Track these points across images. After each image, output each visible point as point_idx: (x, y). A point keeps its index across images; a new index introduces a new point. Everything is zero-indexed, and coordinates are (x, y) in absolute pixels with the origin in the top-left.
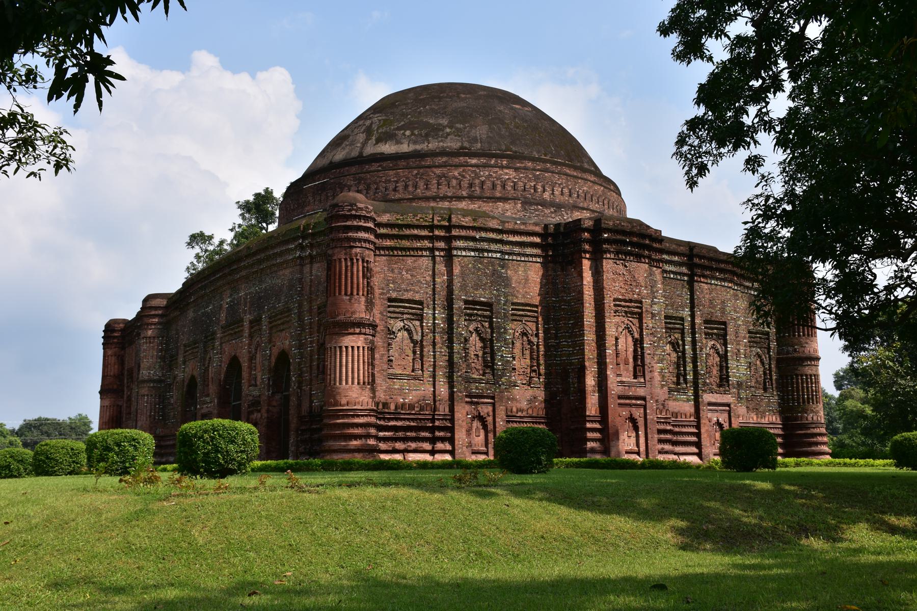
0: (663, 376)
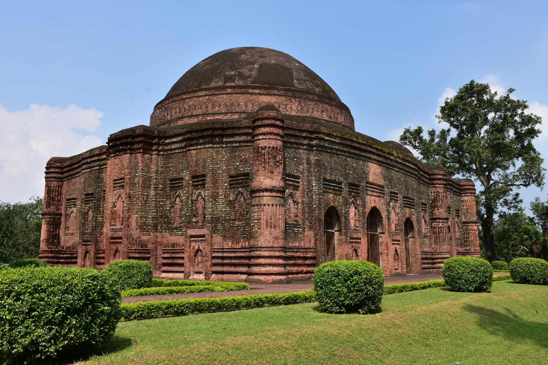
0: (137, 223)
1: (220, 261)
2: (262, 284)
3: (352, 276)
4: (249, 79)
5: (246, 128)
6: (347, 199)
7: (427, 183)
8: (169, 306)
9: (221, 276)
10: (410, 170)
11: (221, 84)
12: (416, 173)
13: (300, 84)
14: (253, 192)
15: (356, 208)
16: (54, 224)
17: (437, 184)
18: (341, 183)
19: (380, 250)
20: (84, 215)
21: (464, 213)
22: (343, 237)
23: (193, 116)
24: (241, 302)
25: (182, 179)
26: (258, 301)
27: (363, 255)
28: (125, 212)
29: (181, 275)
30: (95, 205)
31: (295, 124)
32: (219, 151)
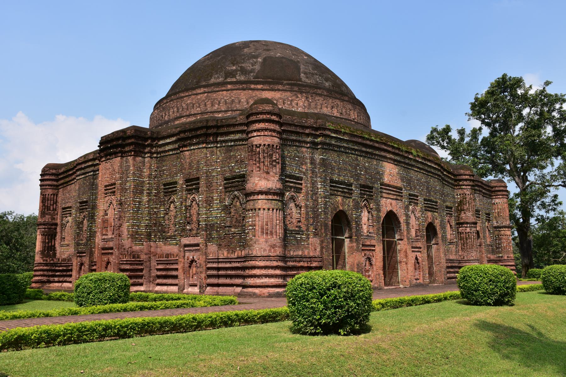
0: (129, 231)
1: (215, 272)
2: (256, 297)
3: (329, 290)
4: (252, 74)
5: (241, 124)
6: (358, 202)
7: (452, 184)
8: (107, 328)
9: (216, 289)
11: (221, 79)
12: (439, 173)
13: (307, 78)
14: (247, 195)
15: (369, 212)
16: (49, 235)
17: (463, 185)
18: (351, 185)
19: (398, 258)
20: (79, 225)
21: (495, 217)
22: (355, 244)
23: (191, 115)
24: (203, 321)
25: (176, 183)
26: (226, 320)
27: (377, 264)
28: (116, 220)
29: (175, 288)
30: (89, 214)
31: (296, 120)
32: (213, 152)
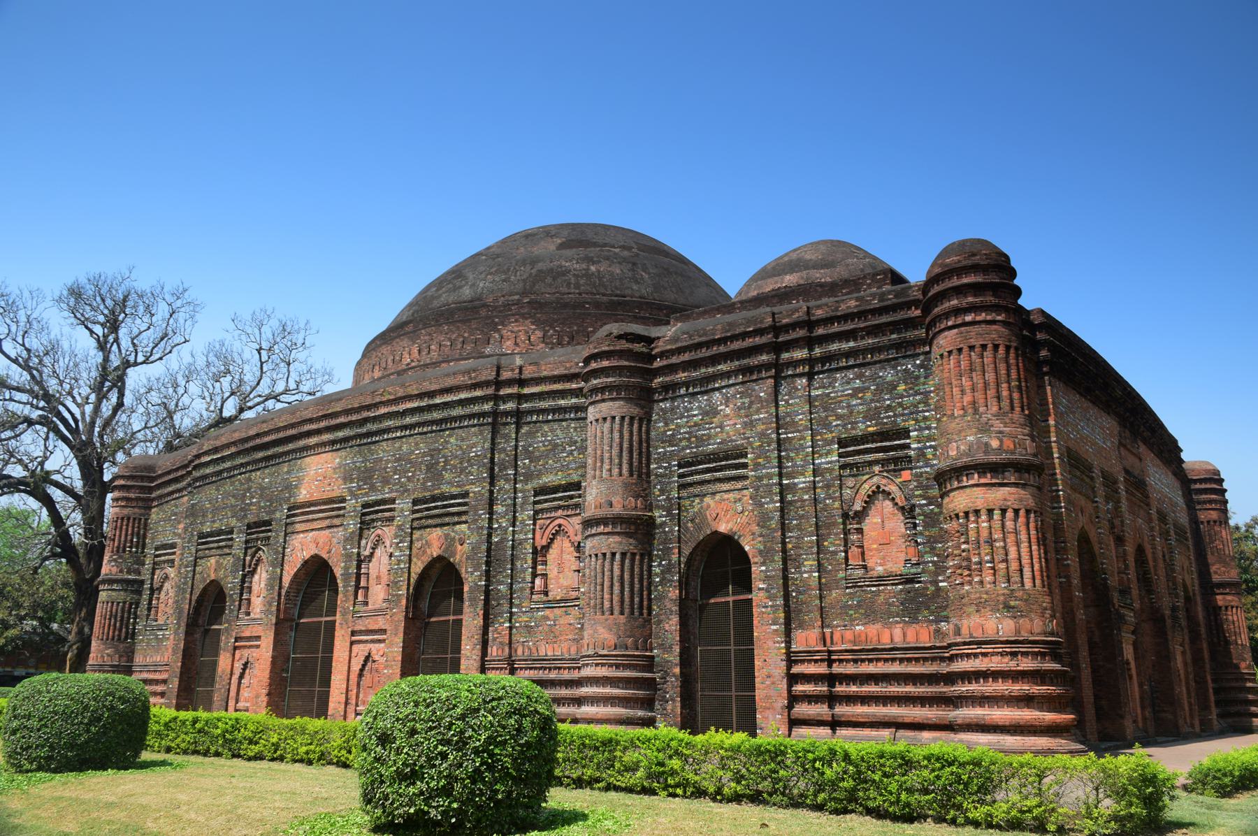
10: (415, 419)
